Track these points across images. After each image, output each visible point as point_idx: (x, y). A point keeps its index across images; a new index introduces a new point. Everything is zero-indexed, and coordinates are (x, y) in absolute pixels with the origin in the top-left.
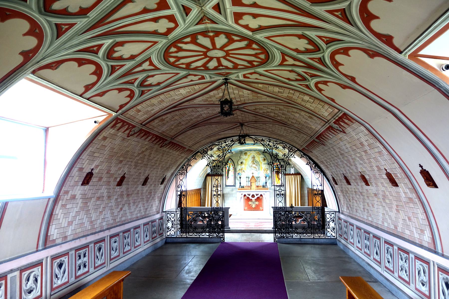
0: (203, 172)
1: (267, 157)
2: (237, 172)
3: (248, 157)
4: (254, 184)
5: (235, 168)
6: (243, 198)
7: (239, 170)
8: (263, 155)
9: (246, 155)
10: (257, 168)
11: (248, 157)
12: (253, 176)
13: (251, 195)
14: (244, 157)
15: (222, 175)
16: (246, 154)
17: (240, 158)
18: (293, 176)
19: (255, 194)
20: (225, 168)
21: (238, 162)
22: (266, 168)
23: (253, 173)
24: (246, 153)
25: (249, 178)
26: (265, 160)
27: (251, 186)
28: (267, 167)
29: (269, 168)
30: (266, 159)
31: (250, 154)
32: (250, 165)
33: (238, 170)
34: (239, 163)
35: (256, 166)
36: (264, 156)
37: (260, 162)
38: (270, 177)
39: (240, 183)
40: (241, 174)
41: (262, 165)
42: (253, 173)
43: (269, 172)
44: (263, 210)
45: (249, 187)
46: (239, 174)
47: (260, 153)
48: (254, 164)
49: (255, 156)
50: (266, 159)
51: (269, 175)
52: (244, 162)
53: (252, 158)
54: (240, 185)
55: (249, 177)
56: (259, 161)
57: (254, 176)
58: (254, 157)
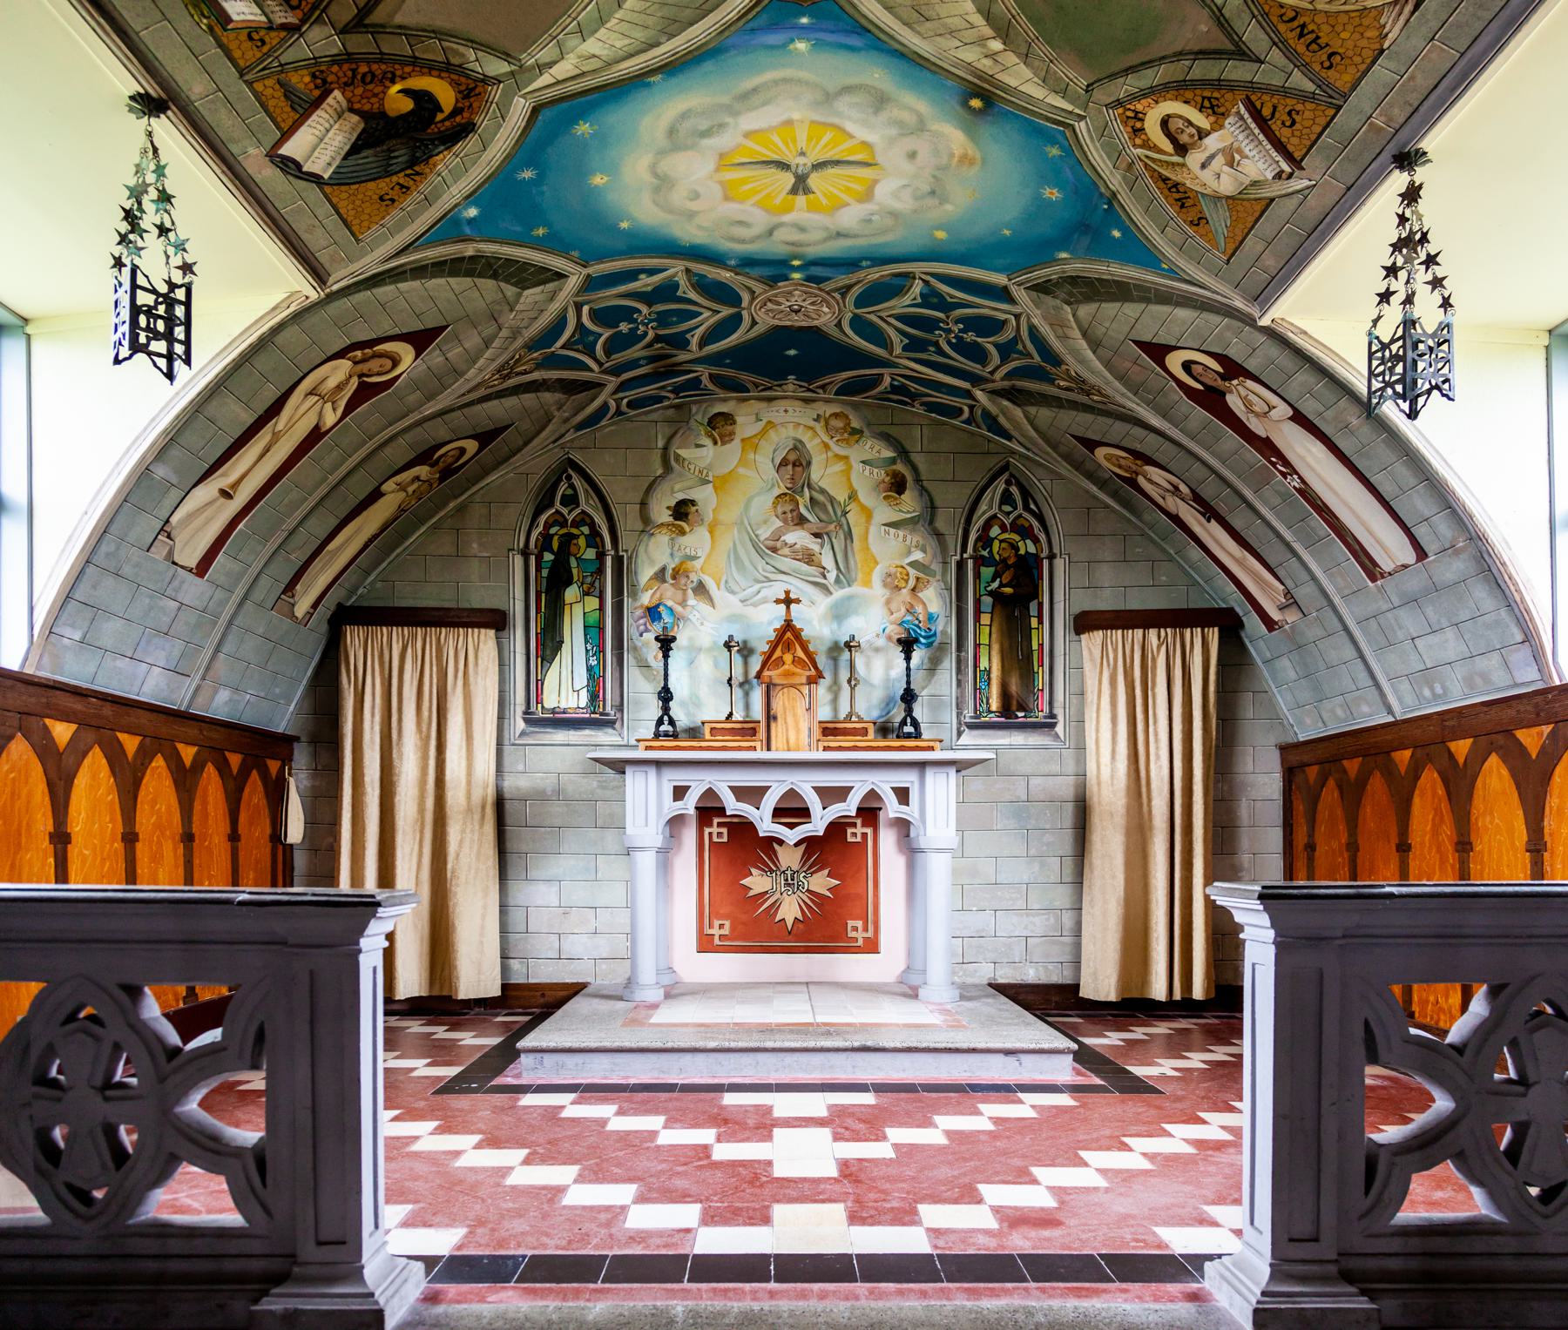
1: (918, 459)
2: (634, 595)
3: (743, 462)
4: (801, 705)
5: (618, 561)
6: (690, 835)
7: (660, 576)
10: (827, 560)
11: (743, 462)
12: (788, 625)
14: (702, 454)
17: (668, 468)
18: (1152, 633)
19: (806, 785)
20: (525, 553)
21: (644, 504)
22: (913, 564)
23: (788, 601)
25: (746, 651)
26: (897, 486)
27: (770, 717)
28: (918, 556)
29: (936, 567)
32: (765, 533)
33: (646, 574)
35: (813, 545)
36: (888, 453)
37: (853, 507)
39: (666, 696)
40: (678, 618)
42: (788, 601)
43: (934, 600)
45: (754, 732)
48: (801, 521)
49: (812, 445)
51: (939, 626)
52: (700, 506)
53: (784, 463)
54: (666, 710)
55: (753, 644)
56: (841, 496)
58: (796, 463)
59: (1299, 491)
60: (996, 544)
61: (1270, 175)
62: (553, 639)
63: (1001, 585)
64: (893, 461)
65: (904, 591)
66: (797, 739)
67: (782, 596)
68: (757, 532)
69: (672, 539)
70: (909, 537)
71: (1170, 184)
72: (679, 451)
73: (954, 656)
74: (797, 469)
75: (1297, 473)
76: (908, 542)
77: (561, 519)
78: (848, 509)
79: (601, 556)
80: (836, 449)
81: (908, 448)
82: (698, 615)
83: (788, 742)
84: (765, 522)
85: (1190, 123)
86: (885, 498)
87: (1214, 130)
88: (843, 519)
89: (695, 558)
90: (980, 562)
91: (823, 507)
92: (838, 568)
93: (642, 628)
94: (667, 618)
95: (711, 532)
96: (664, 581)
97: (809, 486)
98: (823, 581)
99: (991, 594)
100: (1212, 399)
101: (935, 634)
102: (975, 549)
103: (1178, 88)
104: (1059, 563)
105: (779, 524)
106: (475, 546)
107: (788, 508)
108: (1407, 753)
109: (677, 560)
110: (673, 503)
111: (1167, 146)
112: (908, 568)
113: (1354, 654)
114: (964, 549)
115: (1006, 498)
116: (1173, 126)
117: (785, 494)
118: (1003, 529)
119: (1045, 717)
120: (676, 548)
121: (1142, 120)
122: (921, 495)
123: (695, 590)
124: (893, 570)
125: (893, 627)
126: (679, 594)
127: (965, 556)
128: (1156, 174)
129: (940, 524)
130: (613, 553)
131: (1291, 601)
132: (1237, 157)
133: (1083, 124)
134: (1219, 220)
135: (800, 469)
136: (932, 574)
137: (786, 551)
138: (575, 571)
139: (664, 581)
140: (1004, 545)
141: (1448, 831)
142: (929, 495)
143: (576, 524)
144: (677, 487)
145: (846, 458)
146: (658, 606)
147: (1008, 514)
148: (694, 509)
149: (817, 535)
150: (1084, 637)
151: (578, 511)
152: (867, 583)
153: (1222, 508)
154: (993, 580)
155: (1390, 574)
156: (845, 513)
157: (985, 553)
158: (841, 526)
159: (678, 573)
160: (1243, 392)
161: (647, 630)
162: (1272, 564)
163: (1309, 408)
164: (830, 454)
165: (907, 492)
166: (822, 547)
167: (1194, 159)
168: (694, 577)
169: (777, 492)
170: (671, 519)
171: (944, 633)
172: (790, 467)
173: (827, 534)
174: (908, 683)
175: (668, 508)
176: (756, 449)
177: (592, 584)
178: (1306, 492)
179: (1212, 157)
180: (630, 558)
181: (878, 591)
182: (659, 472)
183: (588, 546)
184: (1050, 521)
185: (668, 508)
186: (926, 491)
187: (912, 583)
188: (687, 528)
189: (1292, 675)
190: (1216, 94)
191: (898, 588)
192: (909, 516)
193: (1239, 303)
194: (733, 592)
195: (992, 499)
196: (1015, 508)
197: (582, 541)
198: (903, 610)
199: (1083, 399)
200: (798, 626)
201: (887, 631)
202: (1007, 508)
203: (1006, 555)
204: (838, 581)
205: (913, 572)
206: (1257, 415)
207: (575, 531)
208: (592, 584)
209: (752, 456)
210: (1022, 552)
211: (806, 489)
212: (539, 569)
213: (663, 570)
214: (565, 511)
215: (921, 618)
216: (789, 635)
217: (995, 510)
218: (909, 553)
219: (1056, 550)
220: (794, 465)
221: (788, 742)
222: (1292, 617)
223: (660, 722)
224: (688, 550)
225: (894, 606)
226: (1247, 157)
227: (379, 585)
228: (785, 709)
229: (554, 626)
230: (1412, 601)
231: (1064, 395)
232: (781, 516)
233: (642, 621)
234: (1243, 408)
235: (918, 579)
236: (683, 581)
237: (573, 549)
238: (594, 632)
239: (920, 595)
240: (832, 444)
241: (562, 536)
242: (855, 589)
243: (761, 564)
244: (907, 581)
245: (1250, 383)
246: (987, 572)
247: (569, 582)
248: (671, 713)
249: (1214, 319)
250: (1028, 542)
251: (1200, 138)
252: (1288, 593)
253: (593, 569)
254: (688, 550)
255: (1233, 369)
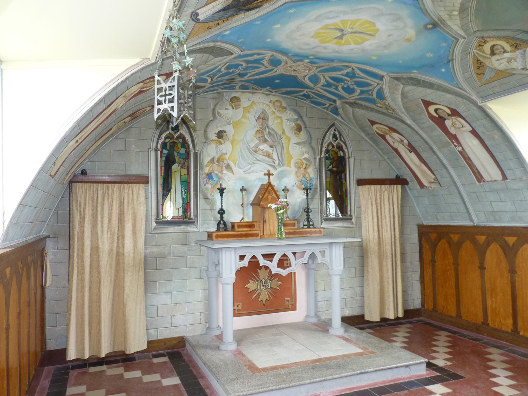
0: (73, 144)
1: (305, 119)
2: (202, 168)
3: (244, 116)
5: (195, 154)
7: (212, 161)
8: (295, 111)
9: (237, 107)
10: (275, 157)
13: (276, 259)
15: (144, 180)
16: (235, 101)
20: (156, 150)
22: (305, 159)
23: (269, 174)
24: (237, 99)
28: (306, 156)
29: (312, 160)
30: (303, 127)
31: (251, 106)
32: (252, 145)
33: (206, 160)
34: (213, 136)
35: (270, 150)
36: (295, 117)
38: (316, 189)
39: (222, 212)
40: (219, 178)
41: (290, 149)
42: (269, 174)
43: (312, 173)
44: (294, 308)
46: (209, 176)
47: (284, 105)
48: (265, 141)
49: (269, 112)
50: (303, 127)
51: (314, 183)
52: (228, 133)
53: (259, 118)
54: (222, 218)
56: (279, 132)
57: (273, 183)
58: (263, 118)
59: (460, 152)
60: (331, 152)
61: (520, 68)
62: (167, 186)
63: (333, 167)
64: (297, 120)
65: (302, 169)
66: (274, 230)
67: (267, 173)
68: (249, 145)
69: (217, 146)
70: (303, 149)
71: (479, 62)
72: (219, 111)
73: (319, 193)
74: (263, 120)
75: (461, 146)
76: (303, 151)
77: (171, 136)
78: (282, 137)
79: (188, 153)
80: (278, 114)
81: (302, 115)
82: (227, 177)
83: (270, 231)
84: (252, 140)
85: (503, 48)
86: (295, 133)
87: (511, 52)
88: (280, 141)
89: (226, 154)
90: (327, 158)
91: (273, 135)
92: (279, 159)
93: (205, 182)
94: (215, 178)
95: (232, 144)
96: (214, 163)
97: (268, 128)
98: (274, 164)
99: (330, 170)
100: (440, 121)
101: (312, 185)
102: (325, 155)
103: (507, 39)
104: (351, 160)
105: (257, 141)
106: (133, 146)
107: (261, 135)
108: (483, 238)
109: (219, 155)
110: (217, 132)
111: (489, 52)
112: (303, 160)
113: (461, 202)
114: (321, 154)
115: (335, 136)
116: (495, 48)
117: (259, 130)
118: (333, 146)
119: (349, 216)
120: (218, 149)
121: (486, 43)
122: (307, 133)
123: (226, 167)
124: (298, 161)
125: (299, 182)
126: (220, 169)
127: (322, 156)
128: (476, 58)
129: (313, 144)
130: (193, 151)
131: (437, 181)
132: (513, 60)
133: (463, 40)
134: (488, 75)
135: (265, 121)
136: (311, 162)
137: (260, 152)
138: (176, 158)
139: (214, 163)
140: (333, 152)
141: (504, 265)
142: (310, 133)
143: (178, 138)
144: (219, 125)
145: (281, 118)
146: (211, 173)
147: (335, 141)
148: (225, 134)
149: (271, 147)
150: (360, 187)
151: (179, 133)
152: (289, 165)
153: (419, 150)
154: (330, 165)
155: (488, 182)
156: (281, 138)
157: (327, 155)
158: (280, 143)
159: (219, 160)
160: (454, 120)
161: (207, 183)
162: (433, 169)
163: (479, 130)
164: (275, 116)
165: (302, 132)
166: (273, 151)
167: (494, 58)
168: (225, 162)
169: (257, 129)
170: (216, 138)
171: (315, 184)
172: (261, 120)
173: (275, 146)
174: (308, 204)
175: (215, 133)
176: (248, 111)
177: (184, 163)
178: (463, 153)
179: (503, 59)
180: (200, 153)
181: (293, 169)
182: (211, 119)
183: (182, 147)
184: (348, 145)
185: (215, 133)
186: (309, 132)
187: (304, 166)
188: (223, 142)
189: (427, 203)
190: (521, 43)
191: (300, 168)
192: (303, 141)
193: (474, 97)
194: (241, 168)
195: (330, 136)
196: (337, 139)
197: (179, 145)
198: (302, 176)
199: (385, 111)
200: (273, 185)
201: (296, 184)
202: (334, 139)
203: (334, 156)
204: (279, 164)
205: (305, 162)
206: (455, 128)
207: (177, 141)
208: (184, 163)
209: (247, 114)
210: (339, 155)
211: (267, 128)
212: (161, 156)
213: (213, 158)
214: (173, 133)
215: (308, 179)
216: (270, 188)
217: (331, 140)
218: (303, 155)
219: (350, 155)
220: (263, 119)
221: (270, 231)
222: (433, 186)
223: (219, 223)
224: (223, 151)
225: (298, 175)
226: (516, 62)
227: (89, 163)
228: (269, 217)
229: (168, 182)
230: (496, 191)
231: (379, 109)
232: (258, 139)
233: (205, 180)
234: (451, 125)
235: (306, 164)
236: (221, 163)
237: (176, 148)
238: (185, 184)
239: (307, 170)
240: (276, 111)
241: (171, 143)
242: (285, 168)
243: (251, 157)
244: (303, 165)
245: (459, 119)
246: (329, 162)
247: (174, 162)
248: (224, 219)
249: (460, 99)
250: (341, 152)
251: (504, 53)
252: (436, 179)
253: (185, 157)
254: (223, 151)
255: (455, 113)
